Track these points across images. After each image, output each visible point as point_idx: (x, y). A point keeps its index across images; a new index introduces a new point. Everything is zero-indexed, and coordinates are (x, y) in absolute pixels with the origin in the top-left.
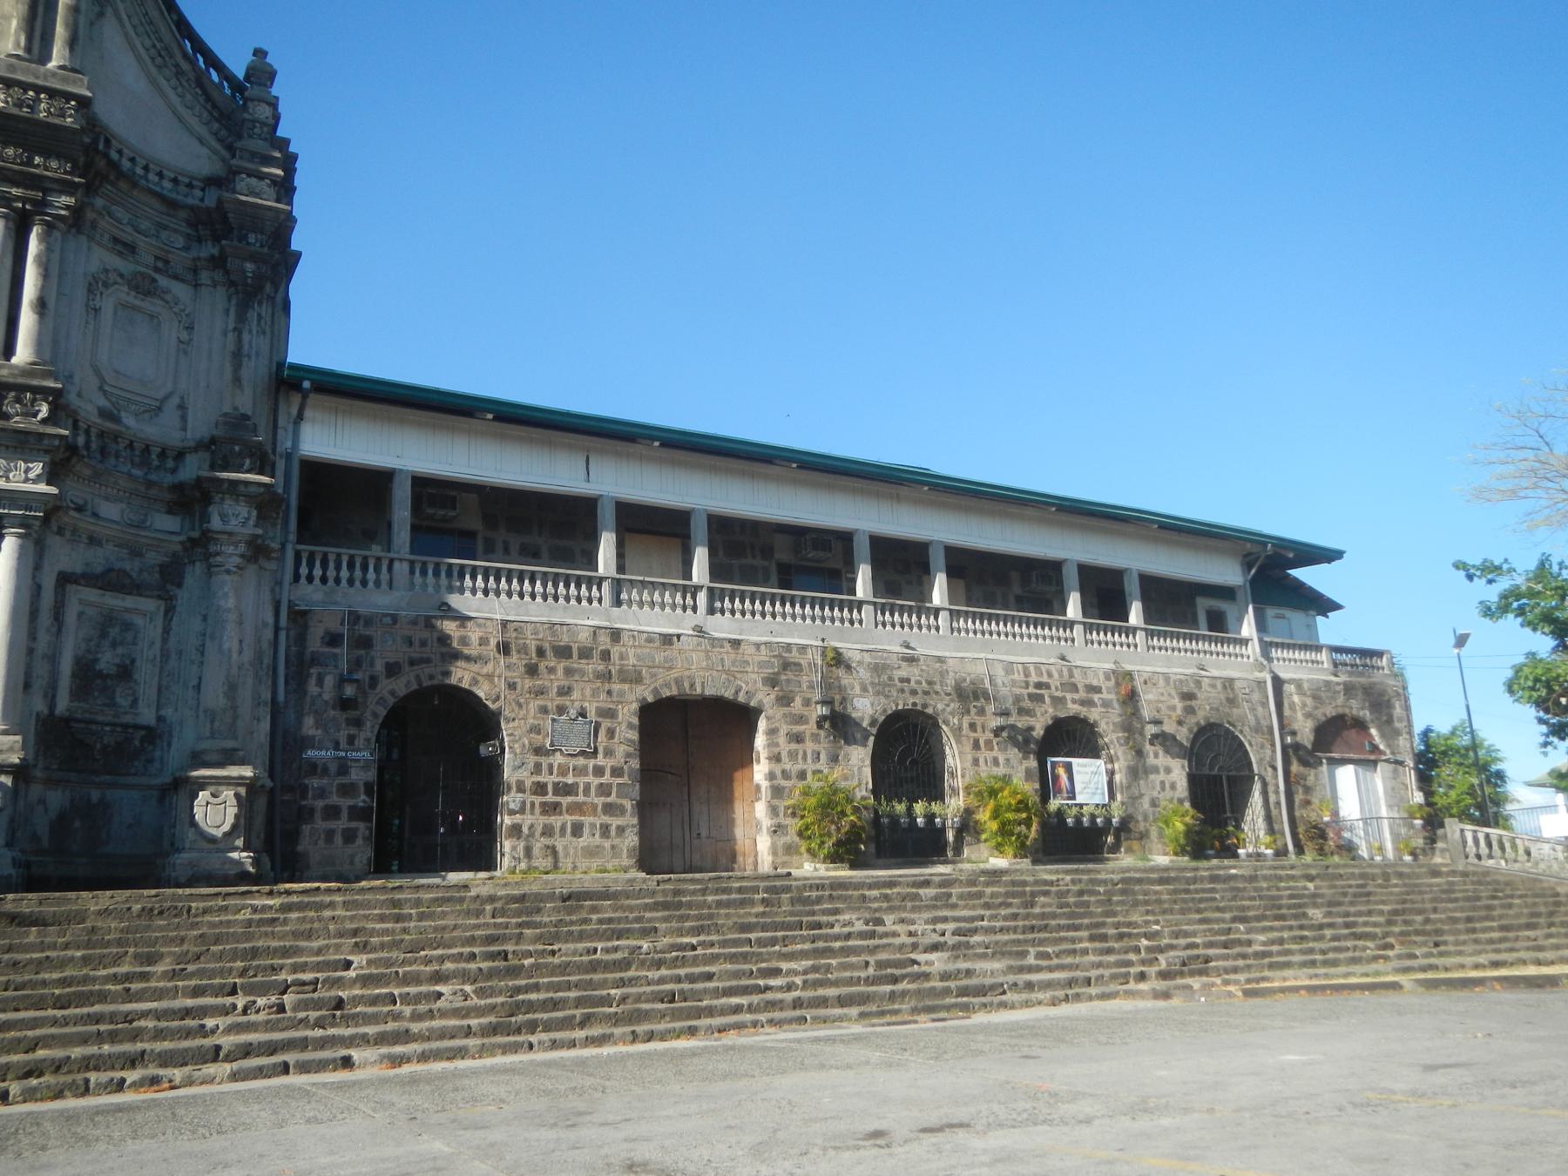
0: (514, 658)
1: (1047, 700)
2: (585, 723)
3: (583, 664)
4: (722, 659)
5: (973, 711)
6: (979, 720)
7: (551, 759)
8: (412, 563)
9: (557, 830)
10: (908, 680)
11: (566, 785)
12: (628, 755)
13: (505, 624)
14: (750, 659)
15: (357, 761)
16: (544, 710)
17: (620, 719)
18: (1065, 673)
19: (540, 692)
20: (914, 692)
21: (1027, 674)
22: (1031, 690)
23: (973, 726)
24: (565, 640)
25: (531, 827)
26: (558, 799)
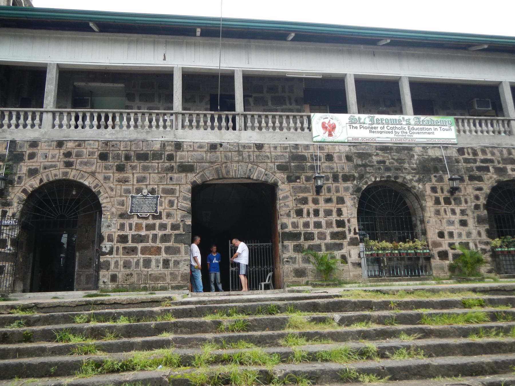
0: (111, 162)
1: (491, 169)
2: (154, 198)
3: (155, 164)
4: (249, 156)
5: (434, 180)
6: (438, 185)
7: (131, 221)
8: (54, 113)
9: (133, 264)
10: (384, 162)
11: (140, 236)
12: (183, 217)
13: (106, 143)
14: (269, 154)
15: (7, 226)
16: (128, 191)
17: (177, 195)
18: (505, 152)
19: (125, 181)
20: (388, 169)
21: (475, 153)
22: (478, 164)
23: (434, 189)
24: (144, 149)
25: (116, 262)
26: (134, 245)
